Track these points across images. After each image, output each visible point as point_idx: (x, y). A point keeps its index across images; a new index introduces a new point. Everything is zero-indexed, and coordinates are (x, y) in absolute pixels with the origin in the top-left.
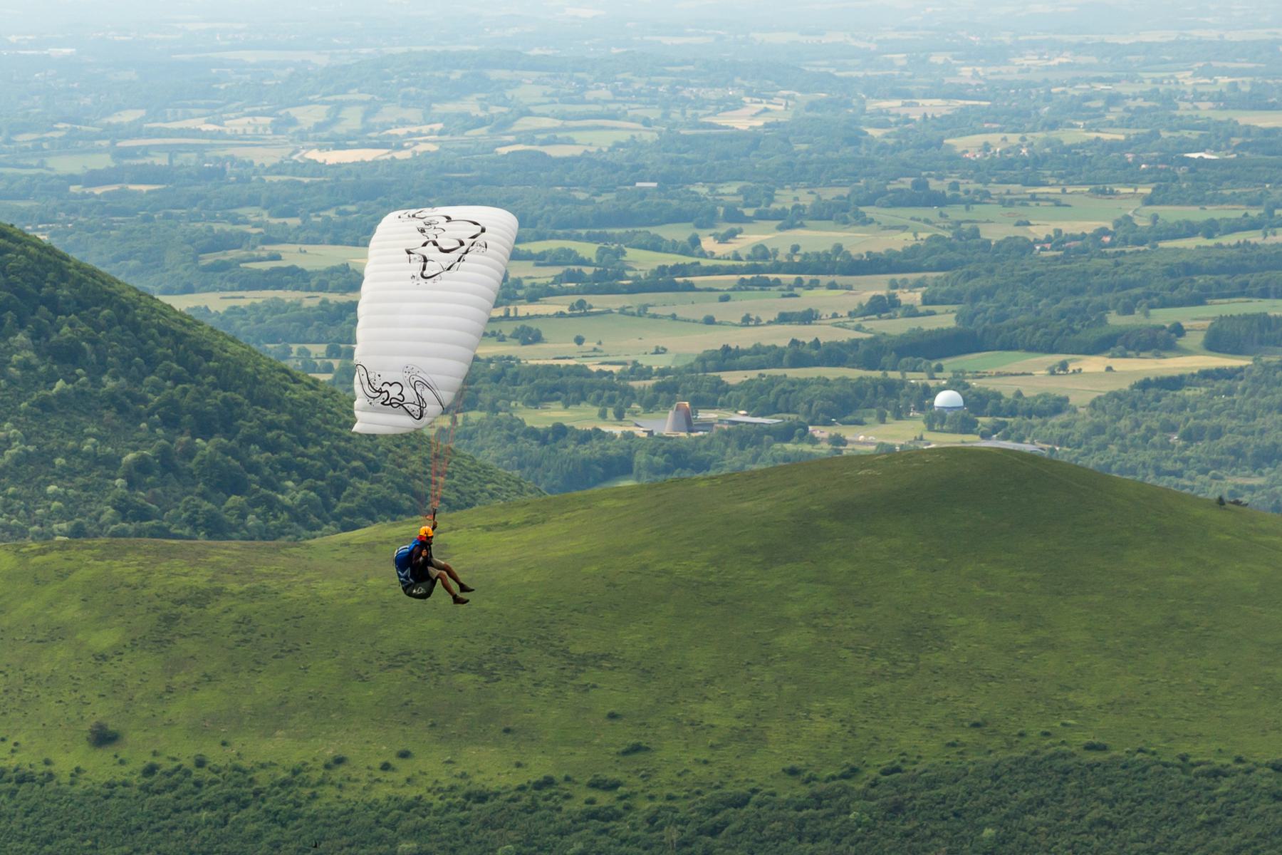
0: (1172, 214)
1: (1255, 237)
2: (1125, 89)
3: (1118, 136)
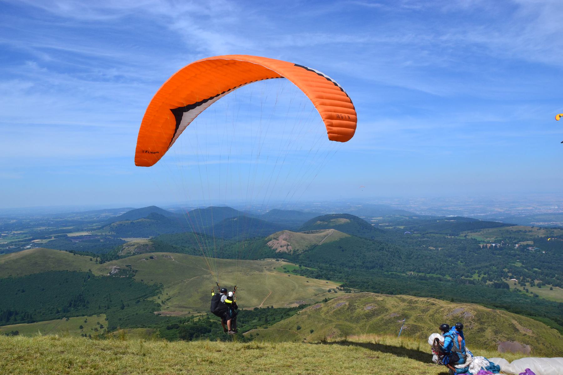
2: (44, 218)
3: (45, 222)
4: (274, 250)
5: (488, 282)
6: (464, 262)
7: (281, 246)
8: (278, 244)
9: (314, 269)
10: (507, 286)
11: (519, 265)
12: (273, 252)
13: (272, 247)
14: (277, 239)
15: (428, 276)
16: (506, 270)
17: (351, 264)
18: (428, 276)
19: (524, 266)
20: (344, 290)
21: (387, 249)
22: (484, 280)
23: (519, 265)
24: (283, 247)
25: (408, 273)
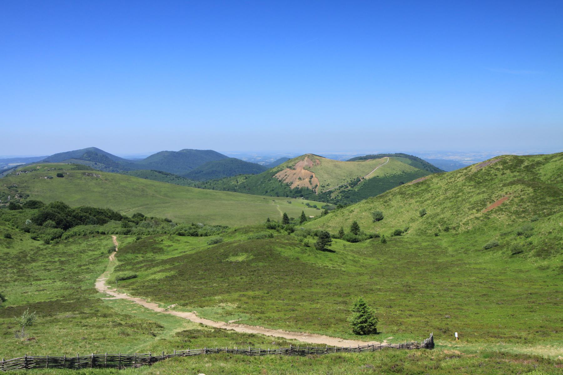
4: (287, 185)
7: (300, 179)
8: (295, 175)
12: (285, 188)
13: (285, 180)
14: (294, 167)
24: (304, 179)
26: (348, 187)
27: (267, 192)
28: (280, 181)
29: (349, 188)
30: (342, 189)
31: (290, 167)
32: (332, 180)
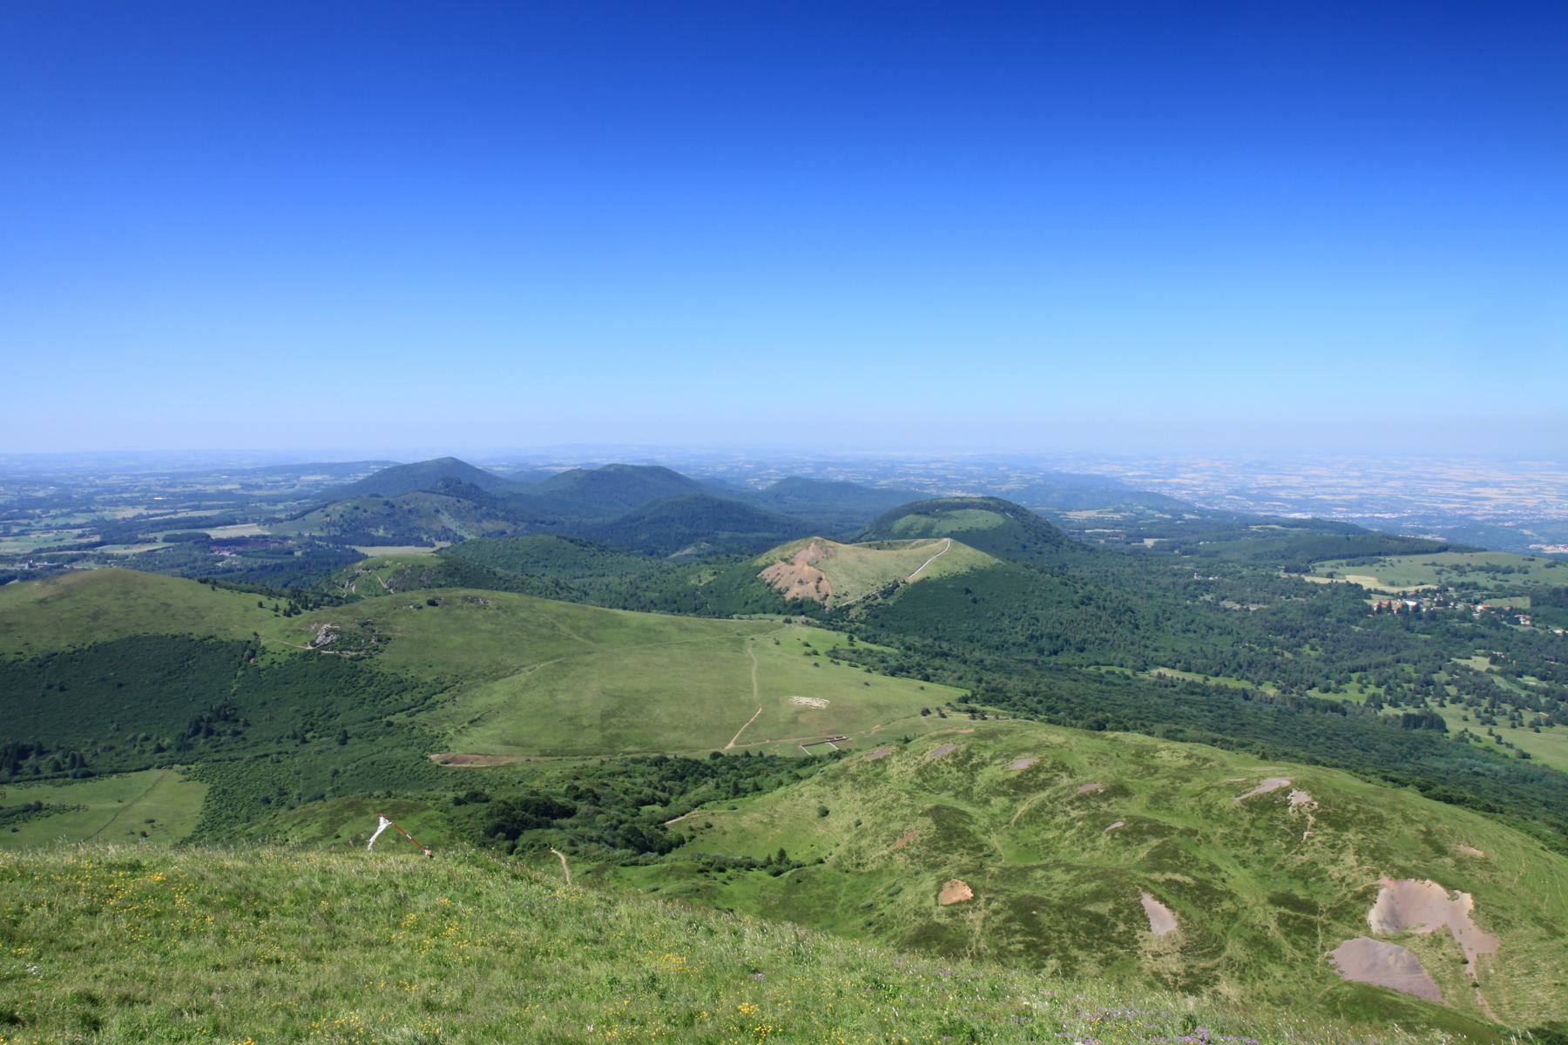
0: (152, 512)
1: (172, 516)
3: (138, 495)
4: (780, 592)
5: (1388, 710)
6: (1320, 649)
7: (801, 582)
9: (888, 650)
10: (1438, 723)
11: (1480, 663)
12: (777, 598)
13: (776, 583)
15: (1213, 681)
16: (1442, 676)
17: (995, 639)
18: (1213, 681)
19: (1496, 668)
20: (967, 711)
21: (1101, 603)
22: (1376, 702)
23: (1480, 663)
25: (1155, 672)
26: (877, 598)
27: (746, 603)
28: (769, 585)
29: (880, 600)
30: (869, 602)
31: (785, 560)
32: (853, 585)
